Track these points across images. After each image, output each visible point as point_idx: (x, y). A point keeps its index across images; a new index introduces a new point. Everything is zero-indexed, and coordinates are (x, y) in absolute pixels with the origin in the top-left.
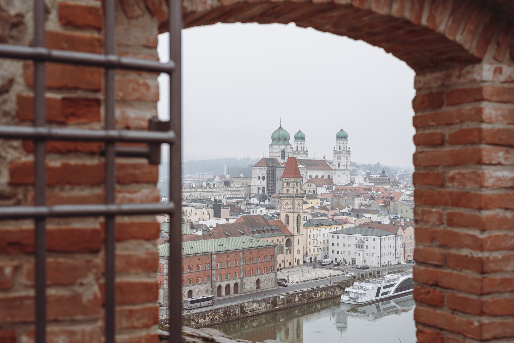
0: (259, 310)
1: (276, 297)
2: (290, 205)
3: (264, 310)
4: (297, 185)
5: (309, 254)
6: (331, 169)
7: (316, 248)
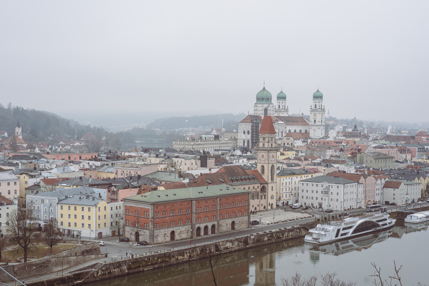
0: (232, 248)
1: (248, 237)
2: (266, 157)
3: (237, 248)
4: (272, 140)
6: (308, 125)
7: (288, 194)
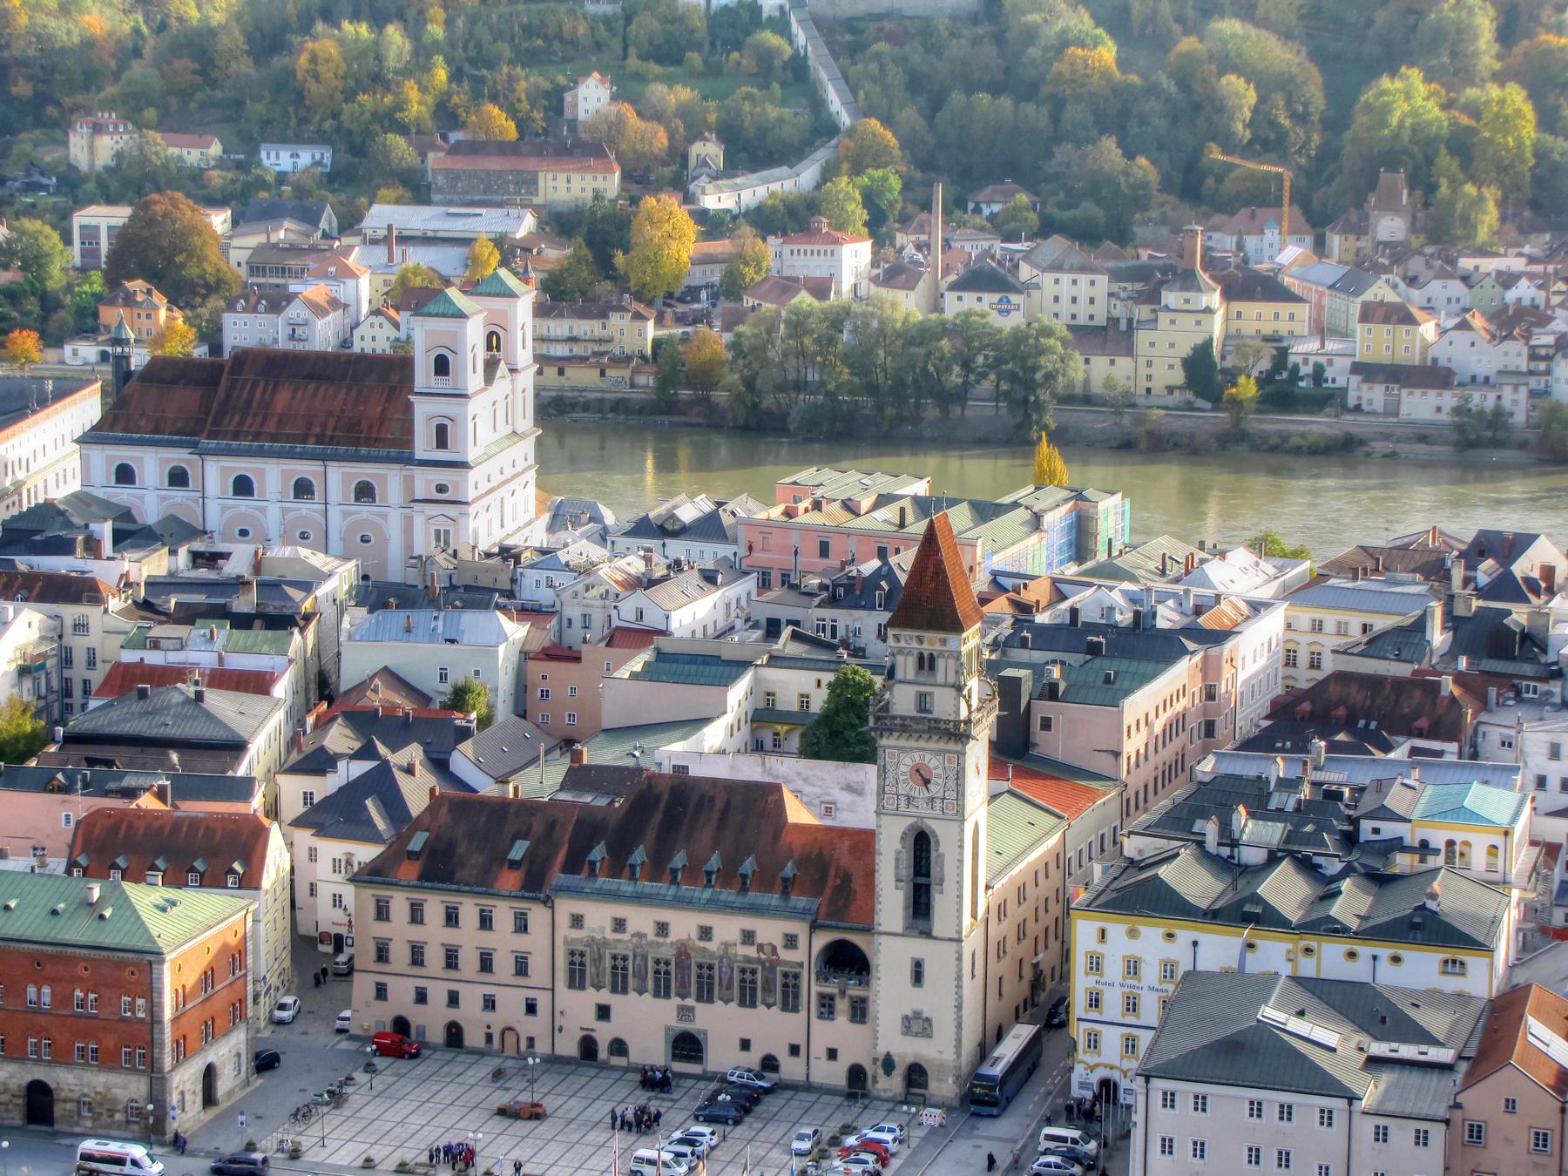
5: (1081, 1055)
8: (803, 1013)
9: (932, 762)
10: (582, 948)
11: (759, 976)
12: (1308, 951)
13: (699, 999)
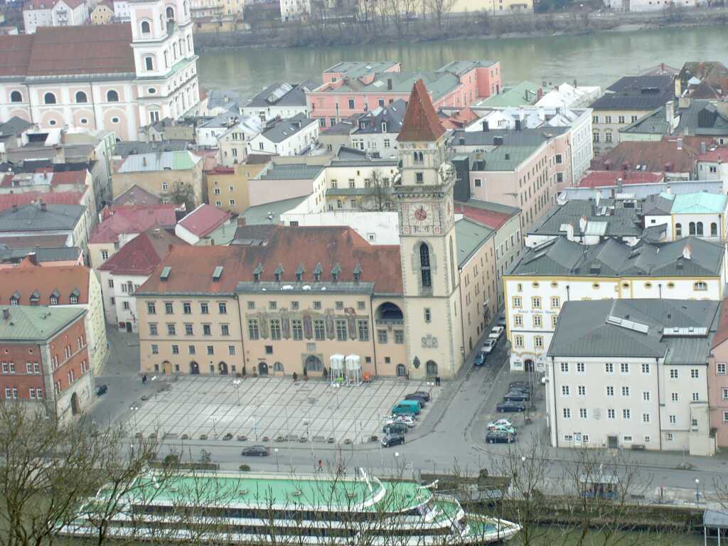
8: (371, 341)
9: (426, 208)
10: (255, 318)
11: (347, 325)
12: (626, 285)
13: (317, 338)
